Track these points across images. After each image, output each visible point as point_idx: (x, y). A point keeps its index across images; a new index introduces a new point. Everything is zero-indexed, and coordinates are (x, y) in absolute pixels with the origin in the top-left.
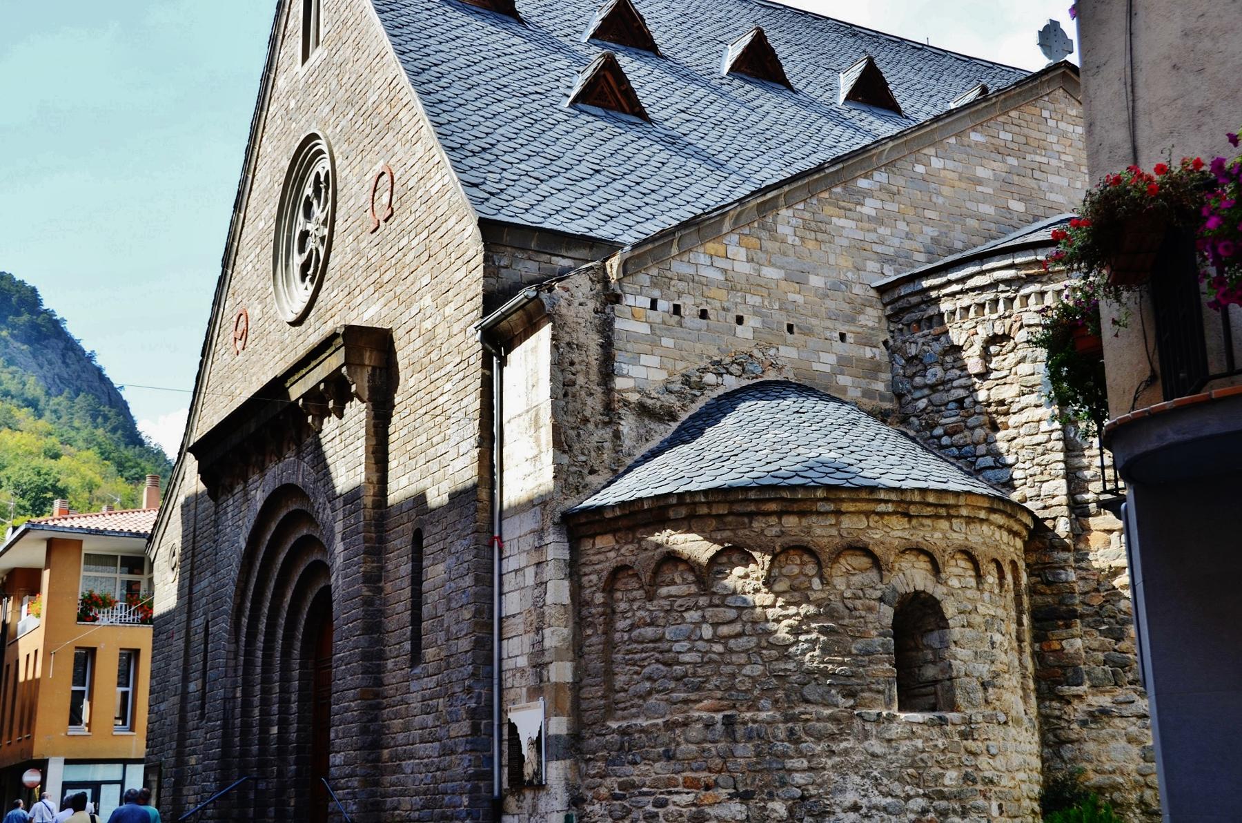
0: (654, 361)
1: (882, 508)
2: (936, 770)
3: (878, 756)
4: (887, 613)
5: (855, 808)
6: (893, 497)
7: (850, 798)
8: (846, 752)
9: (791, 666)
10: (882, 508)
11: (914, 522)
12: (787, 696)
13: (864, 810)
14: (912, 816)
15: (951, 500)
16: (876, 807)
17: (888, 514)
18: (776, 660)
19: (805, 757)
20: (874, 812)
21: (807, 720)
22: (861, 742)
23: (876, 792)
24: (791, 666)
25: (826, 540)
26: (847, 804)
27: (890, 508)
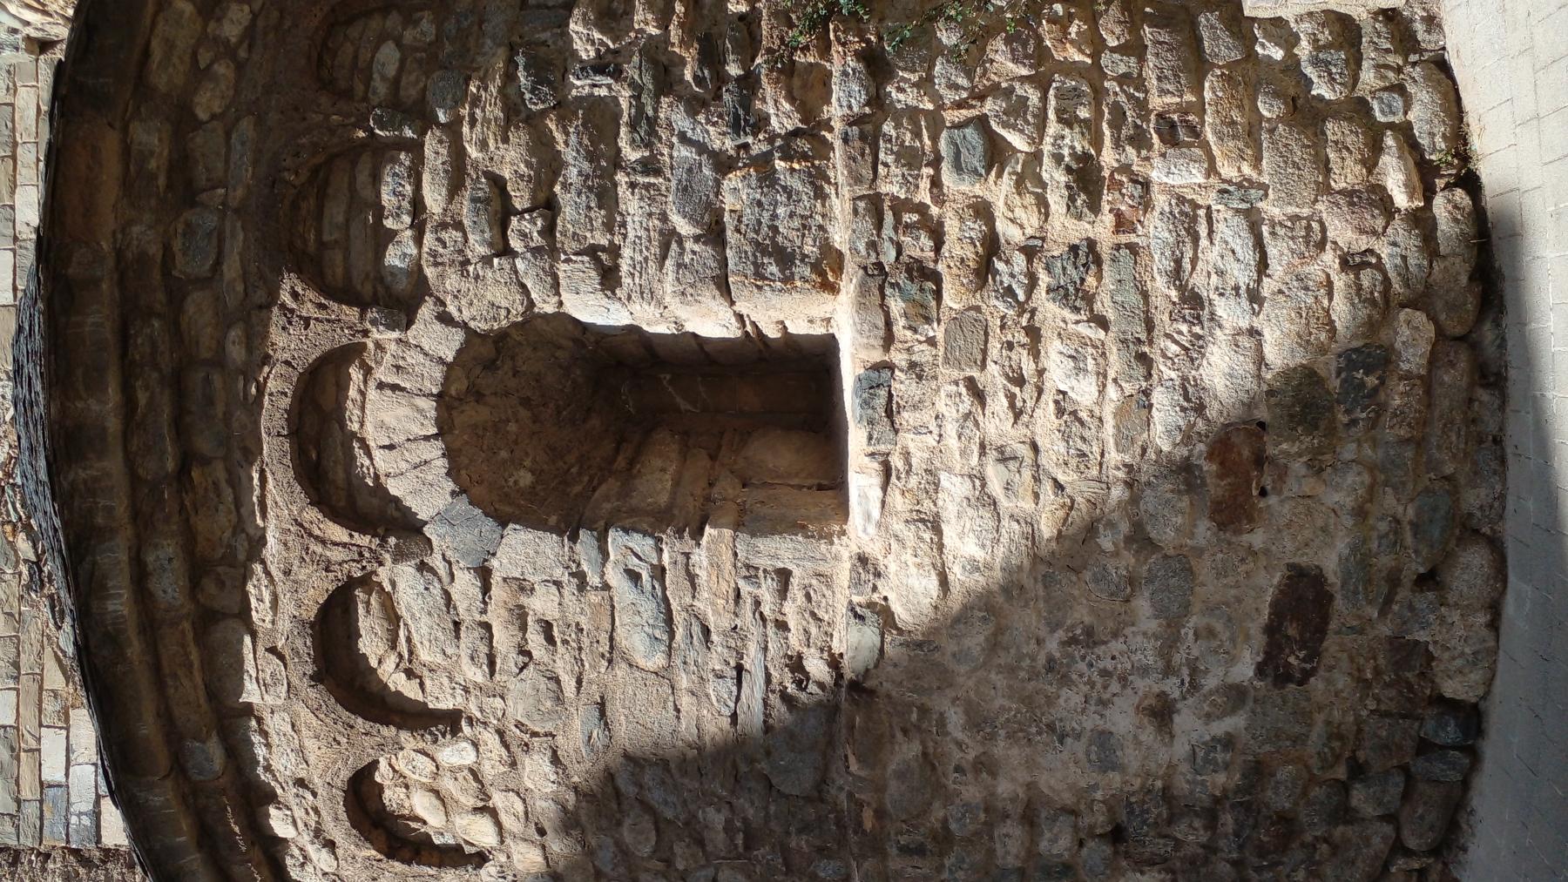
0: (52, 744)
1: (169, 588)
2: (1045, 419)
3: (1000, 630)
4: (524, 551)
5: (1161, 713)
6: (115, 557)
7: (1122, 719)
8: (978, 721)
9: (716, 818)
10: (169, 588)
11: (204, 444)
12: (804, 829)
13: (1172, 687)
14: (1204, 530)
15: (97, 320)
16: (1169, 642)
17: (189, 538)
18: (701, 843)
19: (989, 826)
20: (1178, 658)
21: (880, 814)
22: (946, 679)
23: (1116, 646)
24: (716, 818)
25: (310, 744)
26: (1148, 735)
27: (165, 554)
